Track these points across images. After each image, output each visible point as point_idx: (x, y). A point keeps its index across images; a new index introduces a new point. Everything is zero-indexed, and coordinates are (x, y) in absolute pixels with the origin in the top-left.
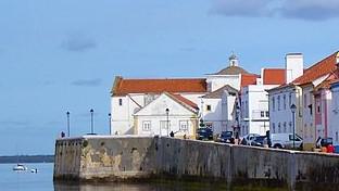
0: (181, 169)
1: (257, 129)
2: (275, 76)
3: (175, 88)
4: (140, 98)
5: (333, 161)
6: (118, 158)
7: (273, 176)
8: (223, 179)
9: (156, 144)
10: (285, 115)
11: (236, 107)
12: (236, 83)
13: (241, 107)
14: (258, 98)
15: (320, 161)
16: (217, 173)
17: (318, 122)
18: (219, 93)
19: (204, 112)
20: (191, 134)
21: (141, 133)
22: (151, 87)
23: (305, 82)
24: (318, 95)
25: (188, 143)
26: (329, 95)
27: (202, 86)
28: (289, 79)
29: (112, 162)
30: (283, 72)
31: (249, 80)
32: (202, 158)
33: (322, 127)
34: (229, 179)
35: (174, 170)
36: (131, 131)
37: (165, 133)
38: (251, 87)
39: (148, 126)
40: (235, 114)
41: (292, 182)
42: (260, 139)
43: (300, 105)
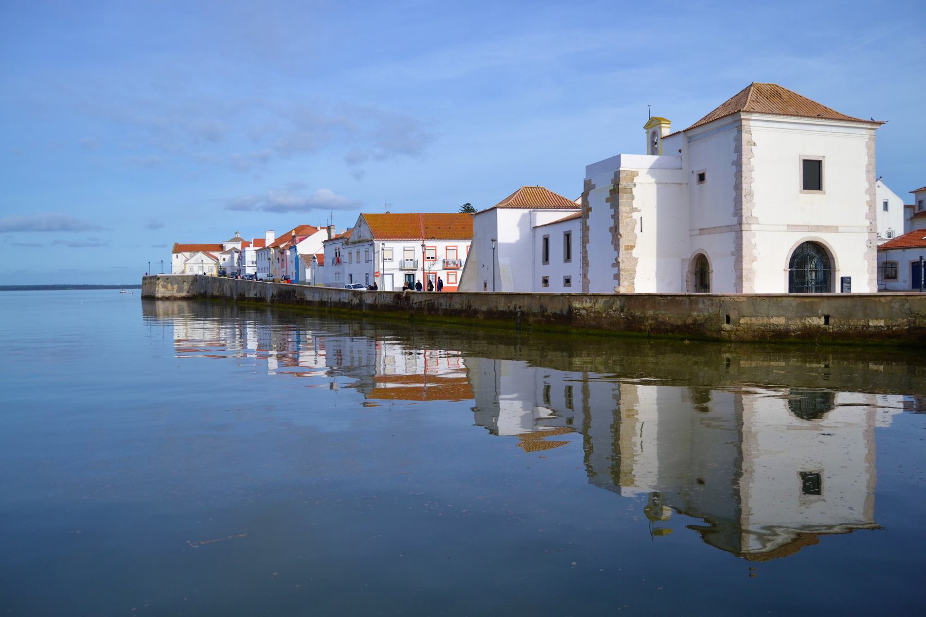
0: (210, 292)
1: (250, 271)
2: (259, 242)
3: (206, 249)
4: (187, 254)
5: (290, 288)
6: (176, 287)
7: (258, 296)
8: (232, 298)
9: (196, 279)
10: (265, 264)
11: (239, 259)
12: (239, 246)
13: (241, 259)
14: (250, 254)
15: (284, 288)
16: (228, 294)
17: (282, 267)
18: (230, 252)
19: (221, 262)
20: (215, 273)
21: (188, 273)
22: (193, 248)
23: (275, 246)
24: (282, 252)
25: (213, 278)
26: (288, 253)
27: (221, 248)
28: (267, 245)
29: (173, 288)
30: (263, 241)
31: (246, 245)
32: (221, 286)
33: (284, 270)
34: (235, 297)
35: (206, 293)
36: (183, 272)
37: (201, 273)
38: (247, 249)
39: (192, 269)
40: (239, 263)
41: (269, 299)
42: (251, 276)
43: (273, 258)
